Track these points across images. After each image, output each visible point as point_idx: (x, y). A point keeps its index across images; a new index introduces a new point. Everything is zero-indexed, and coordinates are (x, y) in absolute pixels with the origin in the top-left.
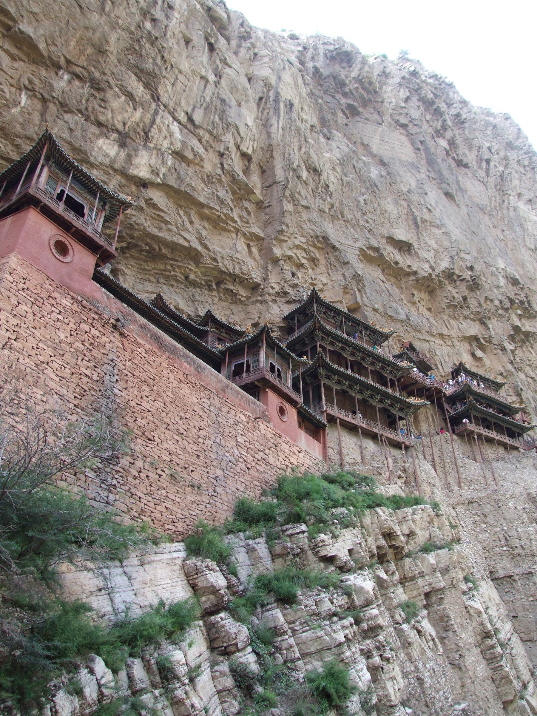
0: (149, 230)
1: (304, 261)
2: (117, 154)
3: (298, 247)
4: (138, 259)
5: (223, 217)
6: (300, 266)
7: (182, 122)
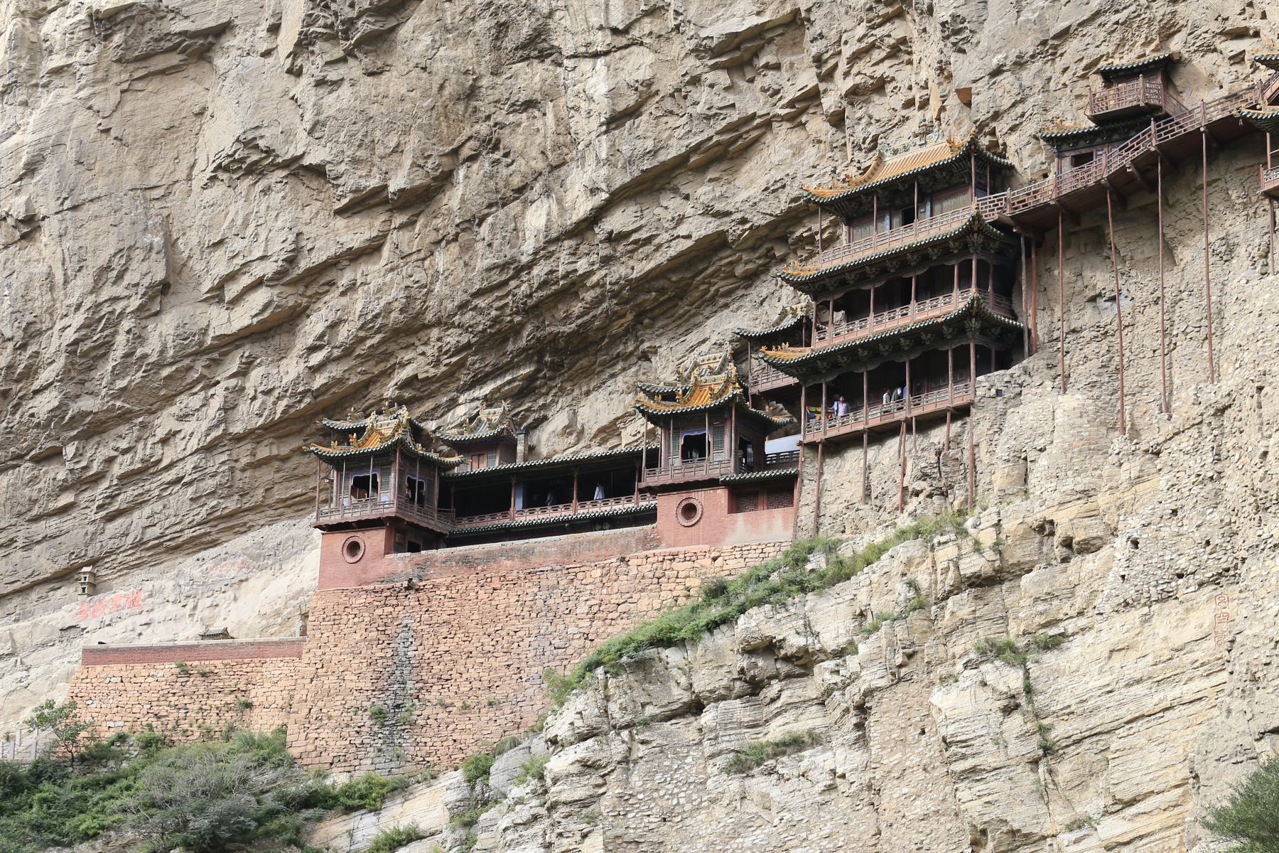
0: (634, 276)
1: (877, 75)
2: (548, 214)
3: (855, 57)
4: (662, 314)
5: (726, 137)
6: (880, 86)
7: (605, 49)
